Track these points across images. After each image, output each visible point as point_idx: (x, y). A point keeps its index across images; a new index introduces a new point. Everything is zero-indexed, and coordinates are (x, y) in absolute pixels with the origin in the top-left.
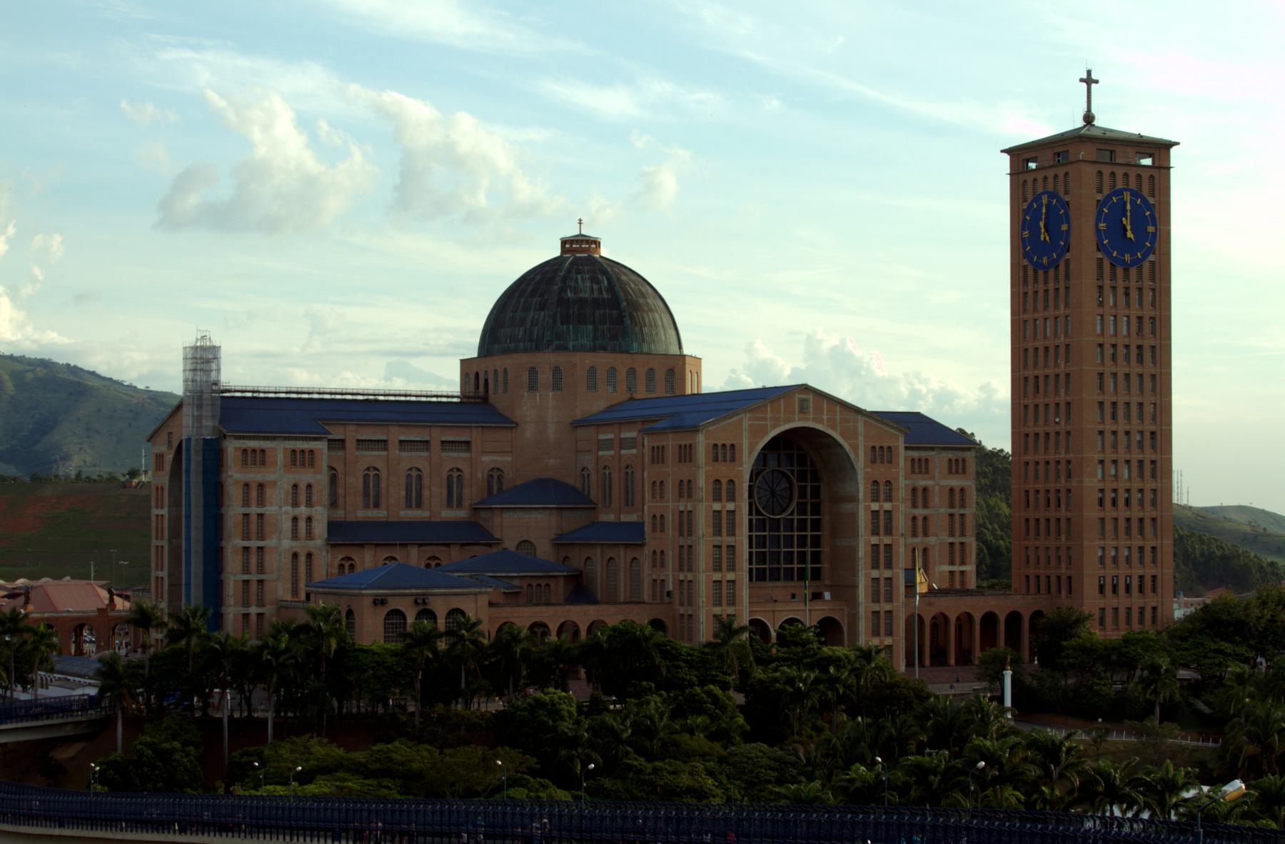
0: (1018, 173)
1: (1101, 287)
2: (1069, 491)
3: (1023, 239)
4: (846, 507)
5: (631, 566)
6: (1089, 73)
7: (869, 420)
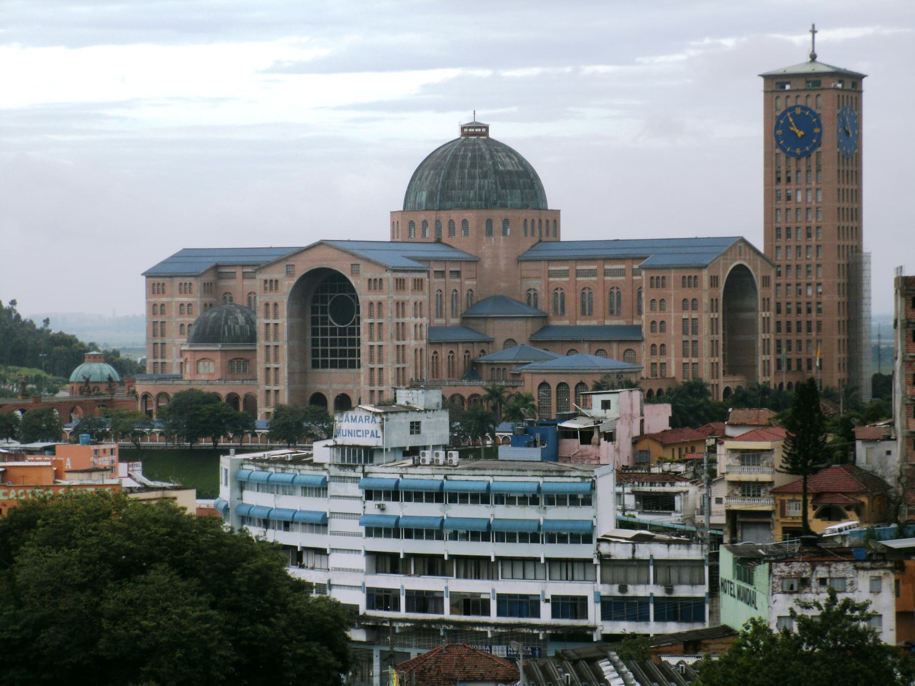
0: (772, 91)
2: (819, 303)
3: (777, 137)
4: (748, 315)
5: (624, 355)
6: (813, 26)
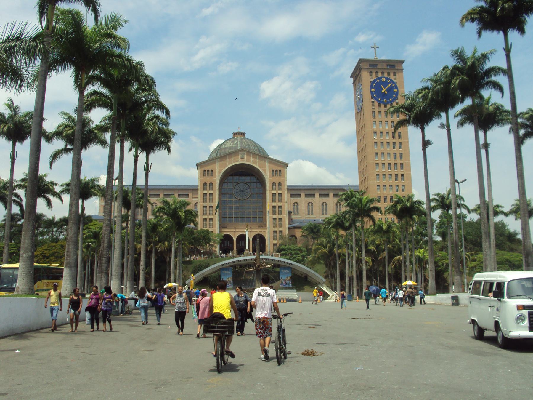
1: (374, 112)
7: (271, 161)
